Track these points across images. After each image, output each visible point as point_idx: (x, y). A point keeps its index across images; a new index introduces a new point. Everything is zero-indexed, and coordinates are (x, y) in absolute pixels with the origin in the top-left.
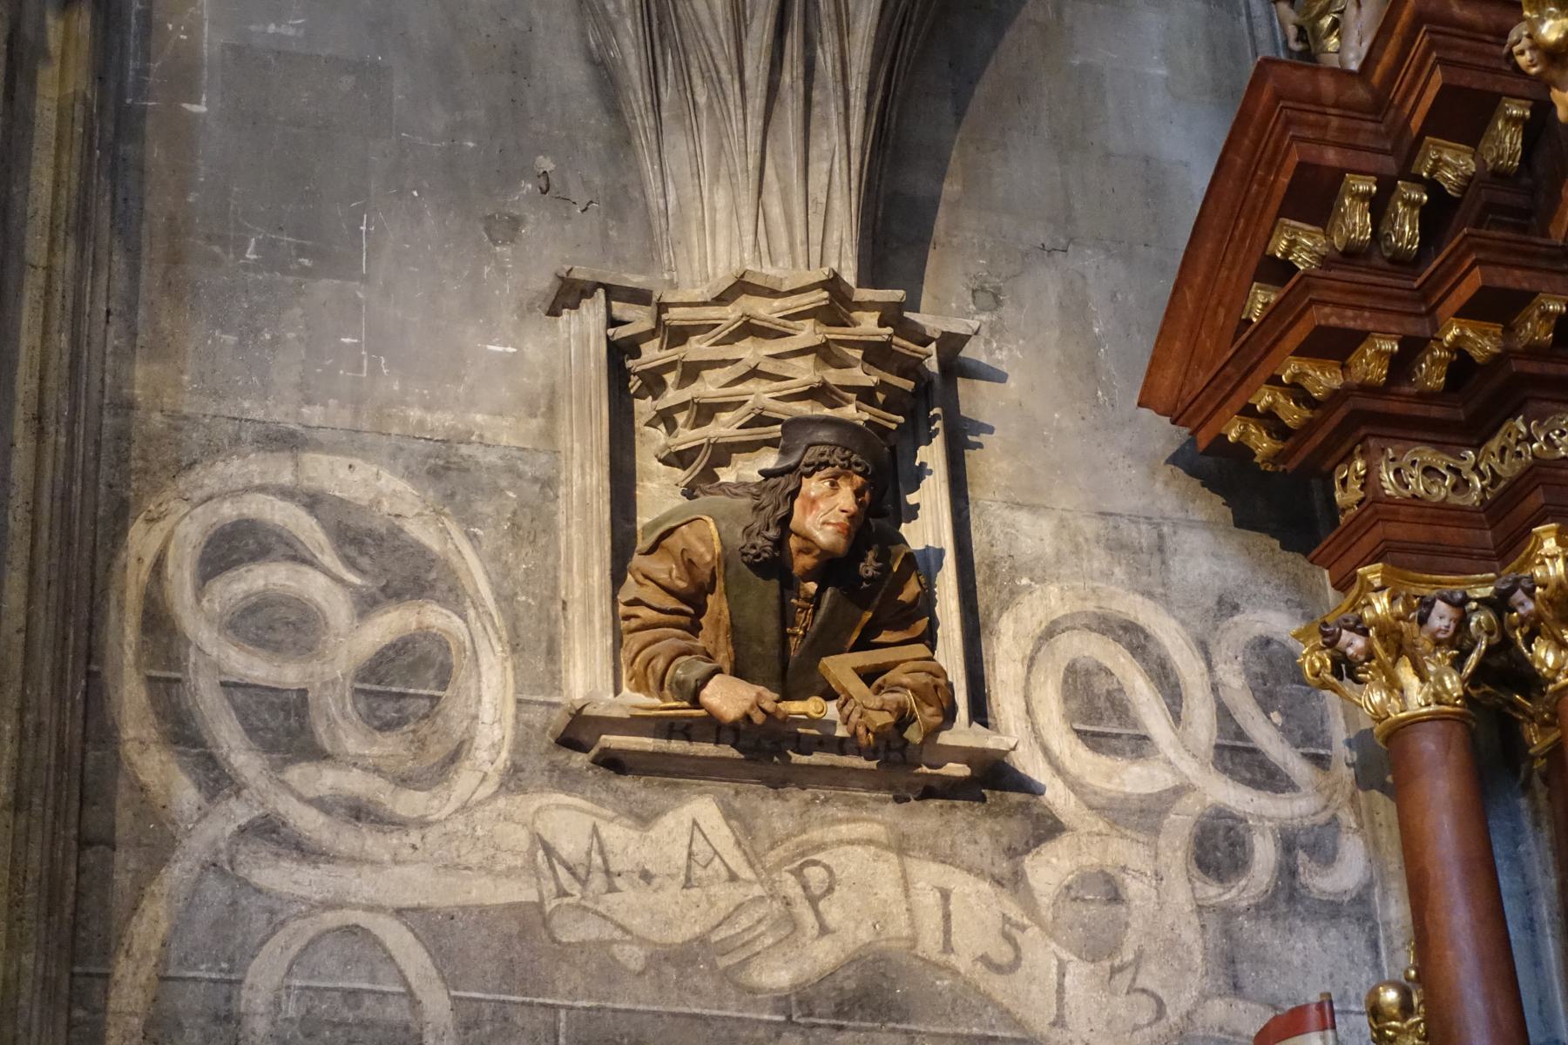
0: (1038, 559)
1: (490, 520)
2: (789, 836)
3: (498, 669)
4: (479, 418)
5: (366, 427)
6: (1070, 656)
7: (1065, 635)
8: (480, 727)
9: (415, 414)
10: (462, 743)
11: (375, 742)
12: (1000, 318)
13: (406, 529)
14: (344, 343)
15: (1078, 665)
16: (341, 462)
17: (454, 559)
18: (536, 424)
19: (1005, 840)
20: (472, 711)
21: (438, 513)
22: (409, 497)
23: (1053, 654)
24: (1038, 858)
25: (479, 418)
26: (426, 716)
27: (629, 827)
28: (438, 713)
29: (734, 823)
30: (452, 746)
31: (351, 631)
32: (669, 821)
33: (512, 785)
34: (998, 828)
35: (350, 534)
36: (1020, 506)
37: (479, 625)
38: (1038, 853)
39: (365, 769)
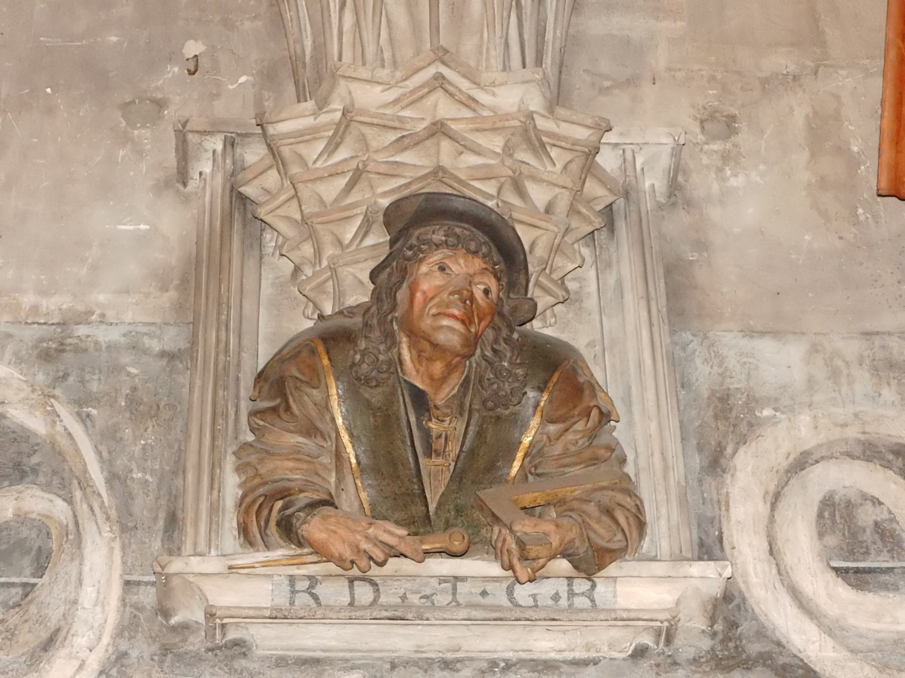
3: (104, 550)
9: (28, 299)
10: (58, 630)
12: (735, 146)
13: (9, 416)
15: (837, 497)
20: (72, 596)
25: (102, 298)
26: (20, 605)
28: (31, 601)
30: (45, 635)
36: (763, 334)
37: (85, 506)
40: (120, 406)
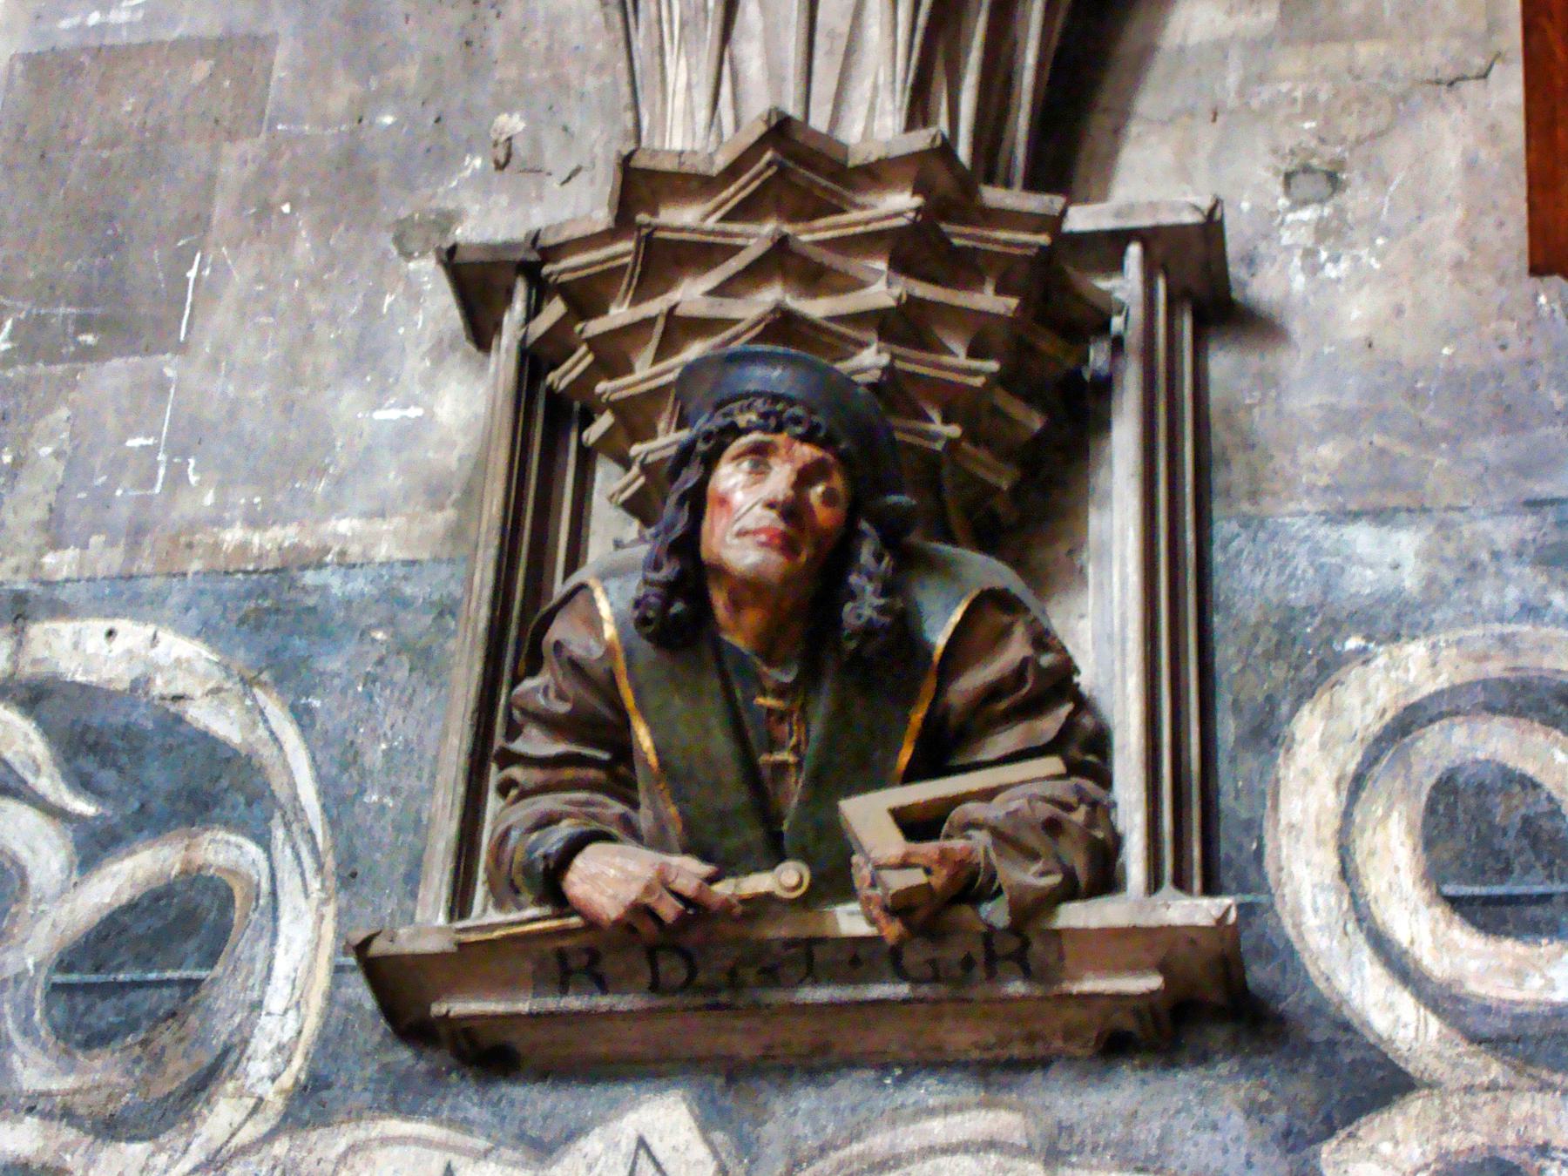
0: (1384, 601)
1: (336, 681)
2: (823, 1150)
3: (309, 919)
4: (344, 526)
5: (147, 566)
6: (1443, 764)
7: (1436, 726)
8: (264, 1020)
9: (232, 536)
11: (71, 1069)
13: (188, 717)
14: (131, 448)
15: (1461, 779)
16: (95, 628)
17: (267, 753)
18: (441, 520)
19: (1280, 1117)
20: (255, 995)
21: (248, 683)
22: (201, 666)
23: (1408, 766)
24: (1351, 1144)
25: (344, 526)
26: (172, 1014)
27: (514, 1164)
29: (719, 1137)
30: (207, 1059)
31: (63, 891)
32: (592, 1144)
33: (306, 1114)
34: (1264, 1096)
35: (91, 738)
36: (1355, 516)
37: (288, 851)
38: (1351, 1136)
39: (47, 1116)
40: (356, 692)
